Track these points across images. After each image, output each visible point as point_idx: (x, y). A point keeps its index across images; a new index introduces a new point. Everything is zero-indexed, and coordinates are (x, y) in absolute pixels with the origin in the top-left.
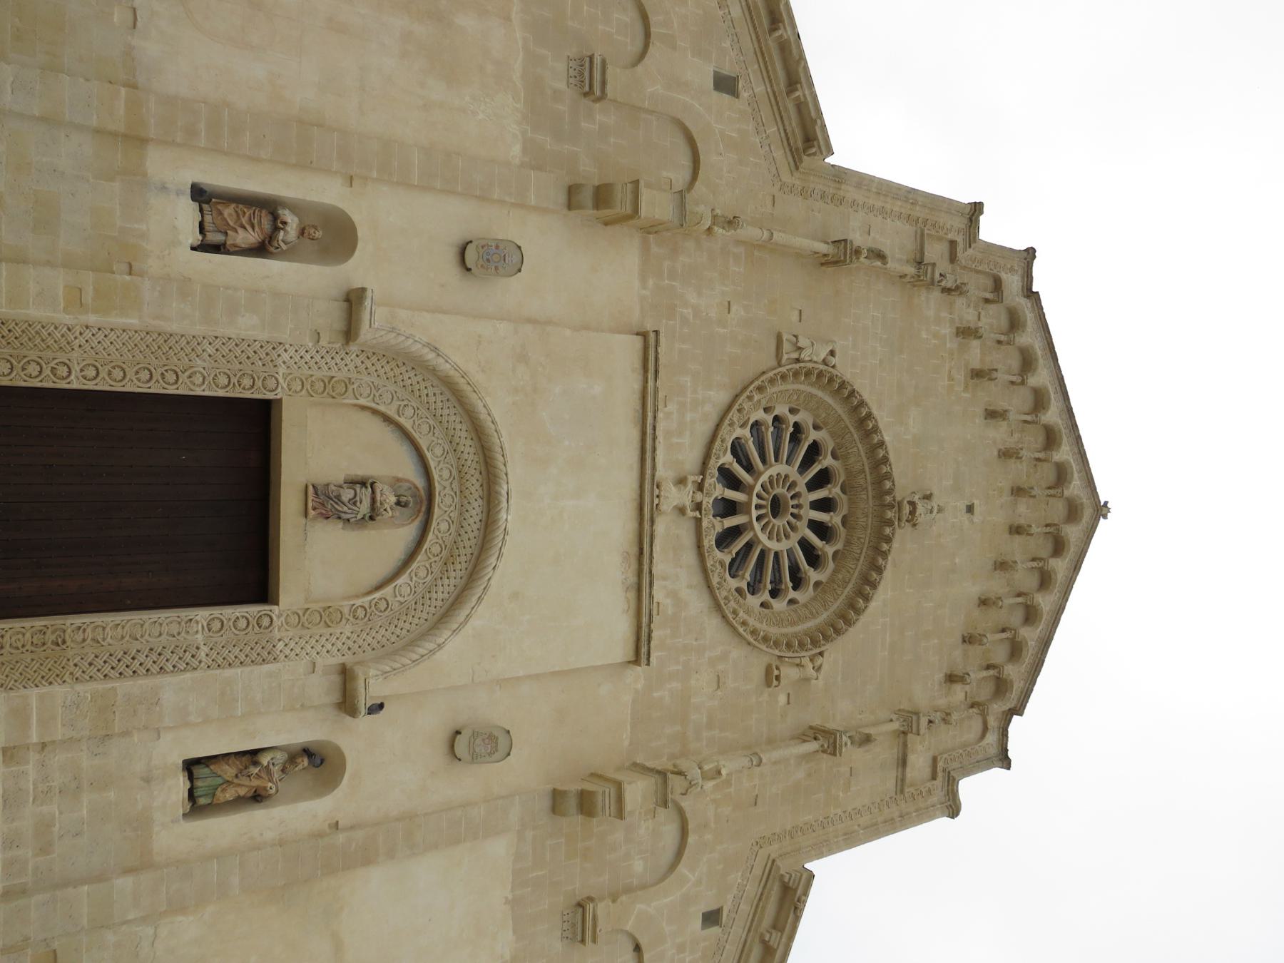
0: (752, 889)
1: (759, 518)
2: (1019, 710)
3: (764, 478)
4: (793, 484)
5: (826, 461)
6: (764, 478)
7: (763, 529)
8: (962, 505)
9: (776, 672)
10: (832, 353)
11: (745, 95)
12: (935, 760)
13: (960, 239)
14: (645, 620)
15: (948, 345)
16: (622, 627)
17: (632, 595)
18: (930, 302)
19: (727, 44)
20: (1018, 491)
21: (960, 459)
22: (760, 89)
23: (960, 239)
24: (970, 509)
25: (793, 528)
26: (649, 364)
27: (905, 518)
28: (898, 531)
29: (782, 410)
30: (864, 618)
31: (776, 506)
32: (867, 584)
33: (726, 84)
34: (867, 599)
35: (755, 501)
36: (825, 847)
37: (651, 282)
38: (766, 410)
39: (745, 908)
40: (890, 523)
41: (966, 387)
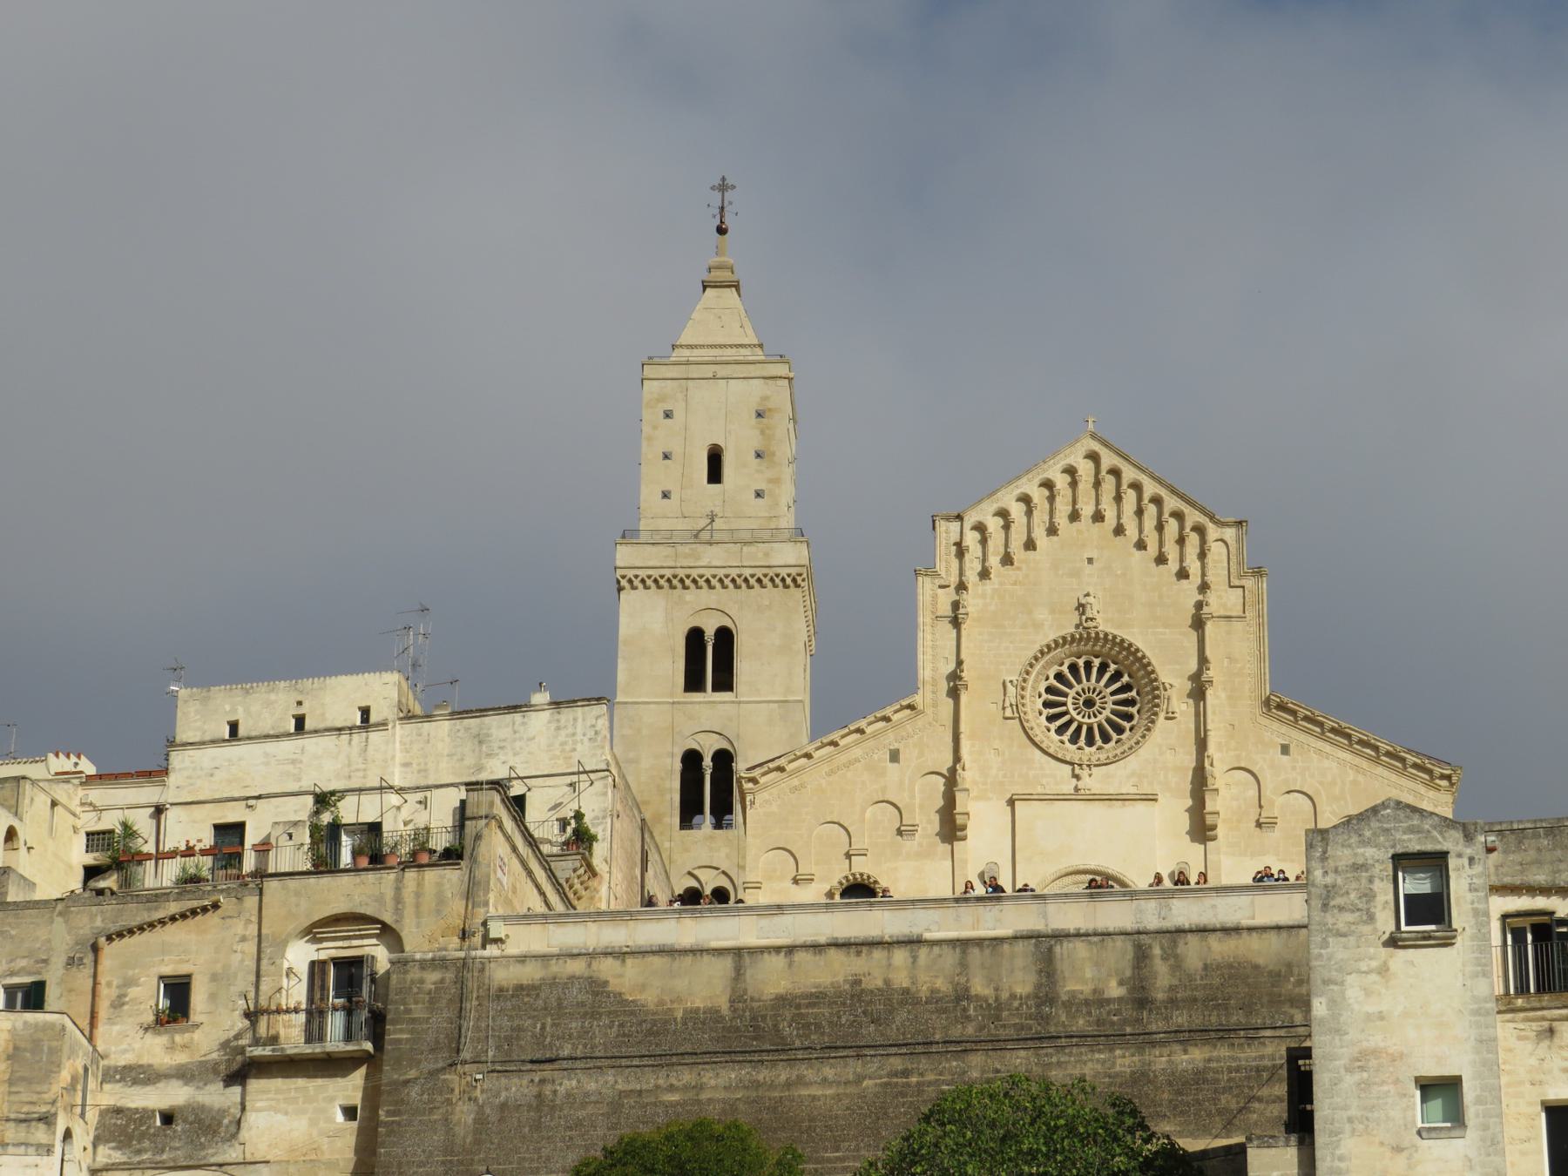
0: (1276, 725)
1: (1095, 716)
3: (1074, 713)
4: (1078, 693)
5: (1065, 669)
6: (1074, 713)
7: (1100, 713)
8: (1088, 569)
9: (1170, 715)
10: (1011, 682)
11: (895, 746)
12: (1231, 587)
13: (938, 582)
14: (1138, 797)
15: (997, 586)
16: (1141, 806)
17: (1127, 803)
18: (972, 603)
19: (876, 757)
21: (1060, 572)
22: (891, 735)
23: (938, 582)
24: (1090, 561)
25: (1100, 692)
26: (1027, 798)
27: (1094, 624)
28: (1100, 628)
29: (1040, 702)
30: (1148, 654)
31: (1089, 703)
33: (895, 756)
34: (1138, 650)
35: (1086, 720)
37: (991, 795)
38: (1041, 714)
39: (1284, 729)
40: (1097, 633)
41: (1019, 569)
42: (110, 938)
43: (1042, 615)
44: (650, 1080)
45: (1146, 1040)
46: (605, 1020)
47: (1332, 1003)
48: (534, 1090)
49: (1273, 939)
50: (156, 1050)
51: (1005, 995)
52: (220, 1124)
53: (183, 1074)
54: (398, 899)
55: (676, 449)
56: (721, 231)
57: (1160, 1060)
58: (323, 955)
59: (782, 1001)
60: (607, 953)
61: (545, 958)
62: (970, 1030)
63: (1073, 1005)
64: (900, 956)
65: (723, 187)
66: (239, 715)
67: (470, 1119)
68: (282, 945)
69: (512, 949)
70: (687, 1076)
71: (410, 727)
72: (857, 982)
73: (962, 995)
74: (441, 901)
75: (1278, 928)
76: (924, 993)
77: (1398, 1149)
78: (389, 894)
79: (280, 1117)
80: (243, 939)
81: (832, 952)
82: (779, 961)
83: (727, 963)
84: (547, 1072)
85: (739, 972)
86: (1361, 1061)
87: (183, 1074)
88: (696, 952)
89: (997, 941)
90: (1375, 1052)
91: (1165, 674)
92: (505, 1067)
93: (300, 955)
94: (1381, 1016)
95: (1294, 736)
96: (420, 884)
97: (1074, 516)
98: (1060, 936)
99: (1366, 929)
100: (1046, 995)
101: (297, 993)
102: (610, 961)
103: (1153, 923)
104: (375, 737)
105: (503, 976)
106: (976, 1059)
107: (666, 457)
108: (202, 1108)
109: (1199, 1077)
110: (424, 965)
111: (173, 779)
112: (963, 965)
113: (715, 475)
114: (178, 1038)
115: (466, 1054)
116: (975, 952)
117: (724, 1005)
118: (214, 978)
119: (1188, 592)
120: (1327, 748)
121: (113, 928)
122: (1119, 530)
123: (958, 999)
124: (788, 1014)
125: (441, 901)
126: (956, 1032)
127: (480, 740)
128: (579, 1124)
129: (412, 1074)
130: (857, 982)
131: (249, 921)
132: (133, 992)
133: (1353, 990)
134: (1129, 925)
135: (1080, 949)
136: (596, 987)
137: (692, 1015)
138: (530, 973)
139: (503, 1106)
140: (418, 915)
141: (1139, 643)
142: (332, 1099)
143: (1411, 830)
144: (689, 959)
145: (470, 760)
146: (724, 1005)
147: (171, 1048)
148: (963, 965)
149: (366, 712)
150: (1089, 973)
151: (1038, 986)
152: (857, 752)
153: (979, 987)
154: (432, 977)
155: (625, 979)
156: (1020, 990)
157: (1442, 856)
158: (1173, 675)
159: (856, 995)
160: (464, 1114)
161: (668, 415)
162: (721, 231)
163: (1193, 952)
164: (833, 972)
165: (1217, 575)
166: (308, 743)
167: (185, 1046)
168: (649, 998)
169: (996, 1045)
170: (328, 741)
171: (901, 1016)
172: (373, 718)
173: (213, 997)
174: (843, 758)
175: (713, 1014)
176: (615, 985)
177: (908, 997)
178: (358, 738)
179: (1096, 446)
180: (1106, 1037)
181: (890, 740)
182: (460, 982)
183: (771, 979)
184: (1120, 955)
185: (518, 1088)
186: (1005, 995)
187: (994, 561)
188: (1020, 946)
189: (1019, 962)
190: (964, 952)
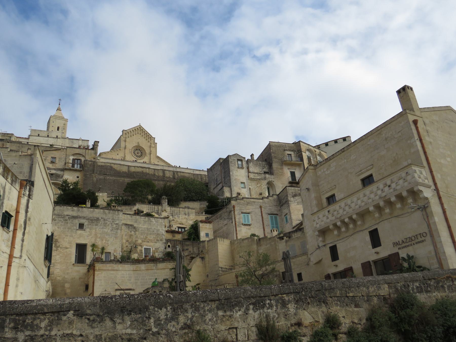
2: (152, 136)
20: (138, 133)
31: (138, 153)
32: (143, 148)
33: (118, 154)
36: (156, 154)
42: (45, 151)
43: (134, 143)
44: (118, 179)
46: (113, 171)
47: (232, 173)
48: (104, 178)
49: (188, 174)
50: (51, 166)
51: (159, 175)
52: (60, 176)
53: (55, 169)
54: (85, 153)
55: (54, 126)
56: (59, 104)
58: (74, 158)
59: (134, 172)
60: (113, 163)
61: (105, 163)
62: (156, 178)
64: (147, 169)
65: (60, 100)
66: (40, 133)
67: (96, 180)
68: (69, 156)
69: (101, 161)
70: (123, 179)
71: (63, 139)
72: (142, 171)
73: (155, 175)
74: (91, 154)
75: (188, 173)
76: (150, 174)
77: (240, 189)
78: (84, 152)
79: (69, 176)
80: (64, 154)
81: (140, 168)
82: (133, 168)
83: (127, 167)
84: (105, 176)
85: (129, 168)
86: (236, 179)
87: (55, 169)
88: (124, 165)
89: (158, 170)
90: (237, 179)
91: (147, 152)
92: (100, 174)
93: (72, 158)
94: (237, 175)
95: (159, 160)
96: (88, 152)
97: (138, 133)
98: (165, 170)
99: (235, 166)
100: (164, 176)
101: (71, 161)
102: (113, 164)
103: (175, 170)
104: (58, 139)
105: (99, 164)
106: (156, 182)
107: (53, 126)
108: (57, 174)
110: (89, 161)
111: (30, 139)
112: (155, 171)
113: (58, 130)
114: (54, 165)
115: (95, 172)
116: (156, 170)
117: (127, 171)
118: (59, 158)
119: (149, 144)
120: (162, 163)
121: (45, 150)
122: (142, 136)
123: (154, 175)
124: (135, 173)
125: (91, 154)
126: (154, 178)
127: (72, 142)
128: (110, 182)
129: (88, 173)
130: (142, 171)
131: (64, 152)
132: (48, 158)
133: (234, 172)
134: (173, 170)
135: (167, 172)
136: (111, 167)
137: (123, 172)
138: (103, 164)
139: (100, 179)
140: (88, 155)
141: (144, 148)
142: (76, 175)
143: (239, 157)
144: (123, 166)
145: (71, 144)
146: (127, 171)
147: (53, 166)
148: (155, 171)
149: (57, 136)
150: (168, 174)
151: (163, 175)
152: (114, 153)
153: (156, 174)
154: (90, 163)
155: (115, 167)
156: (161, 175)
157: (242, 160)
158: (147, 151)
159: (142, 173)
160: (95, 179)
161: (53, 122)
162: (59, 104)
163: (179, 174)
164: (140, 170)
166: (50, 139)
167: (55, 166)
168: (118, 169)
169: (159, 181)
170: (52, 139)
171: (148, 176)
172: (58, 137)
173: (59, 160)
174: (112, 153)
175: (126, 172)
176: (114, 167)
177: (148, 174)
178: (56, 139)
179: (140, 127)
181: (117, 153)
182: (94, 163)
183: (132, 170)
184: (172, 173)
185: (101, 177)
186: (159, 175)
187: (129, 136)
188: (161, 171)
189: (161, 172)
190: (155, 170)
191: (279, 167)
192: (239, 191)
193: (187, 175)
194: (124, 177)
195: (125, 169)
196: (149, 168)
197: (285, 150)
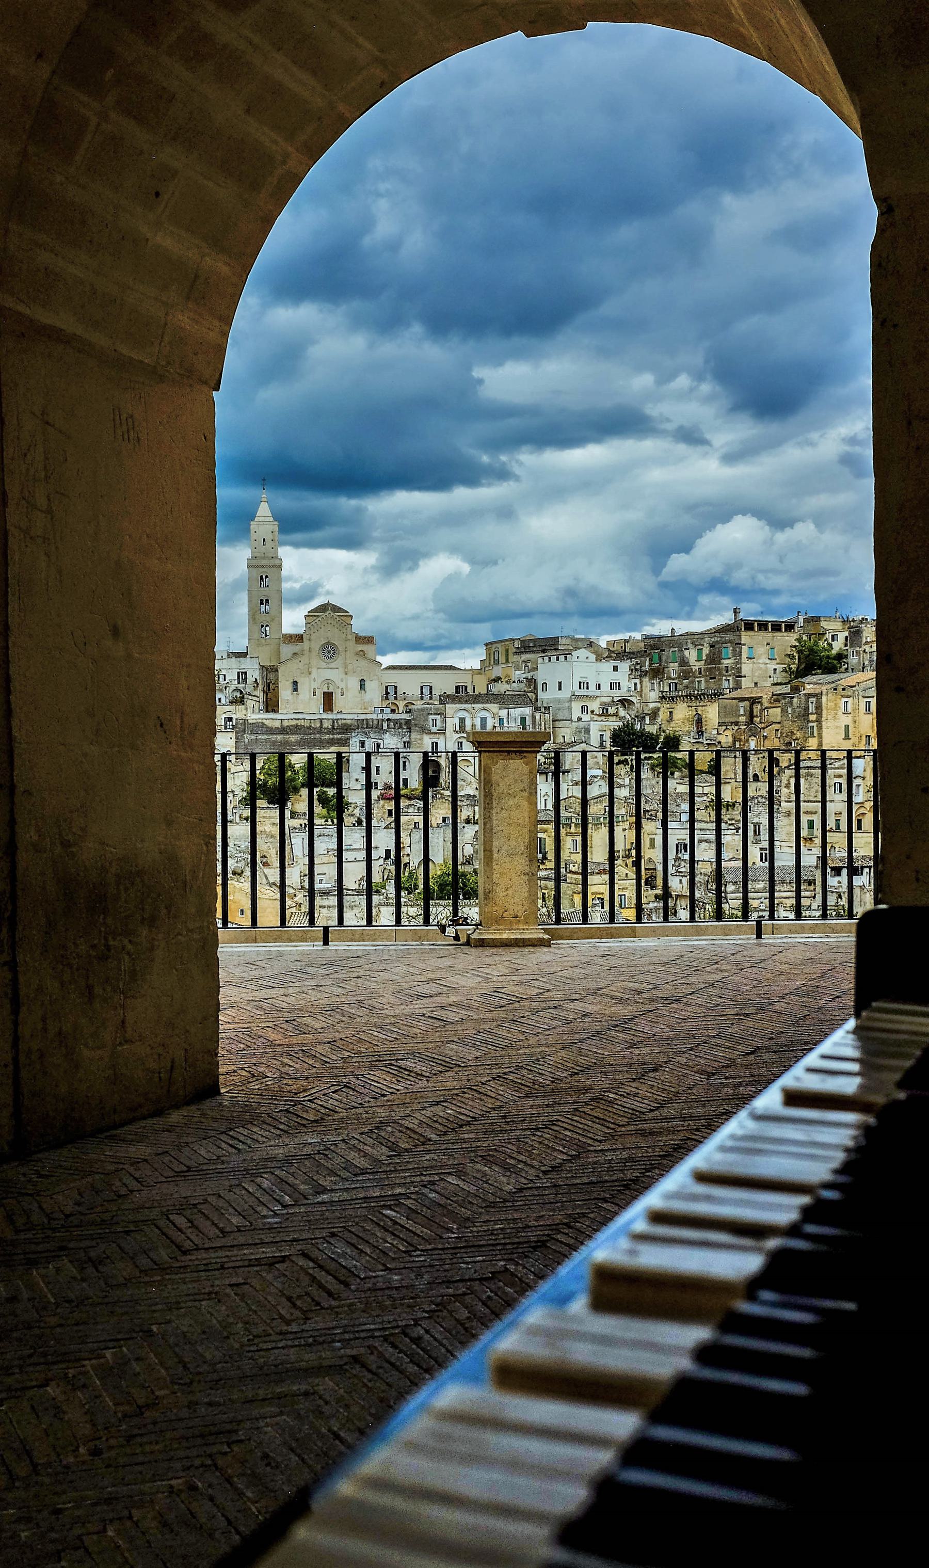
43: (322, 639)
45: (334, 734)
57: (335, 736)
63: (325, 728)
73: (311, 726)
100: (321, 727)
105: (250, 721)
109: (341, 739)
119: (344, 636)
136: (263, 723)
138: (254, 721)
155: (267, 723)
159: (297, 725)
160: (246, 740)
164: (293, 723)
165: (348, 633)
169: (314, 733)
180: (329, 733)
183: (286, 723)
185: (253, 737)
191: (419, 737)
192: (358, 777)
193: (349, 722)
194: (276, 734)
195: (277, 724)
196: (304, 719)
197: (429, 714)
